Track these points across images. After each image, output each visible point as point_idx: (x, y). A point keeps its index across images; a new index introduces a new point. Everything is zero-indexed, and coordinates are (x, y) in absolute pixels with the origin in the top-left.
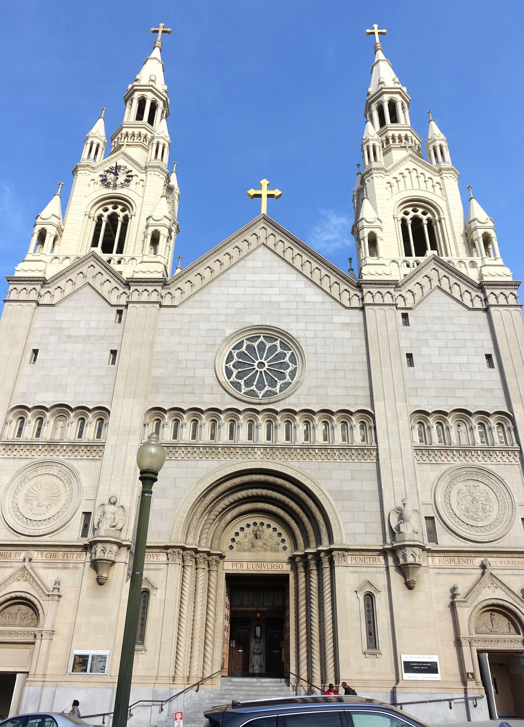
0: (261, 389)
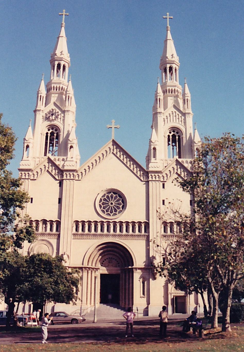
0: (111, 213)
